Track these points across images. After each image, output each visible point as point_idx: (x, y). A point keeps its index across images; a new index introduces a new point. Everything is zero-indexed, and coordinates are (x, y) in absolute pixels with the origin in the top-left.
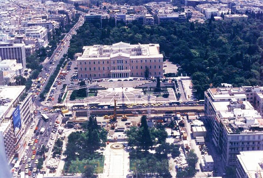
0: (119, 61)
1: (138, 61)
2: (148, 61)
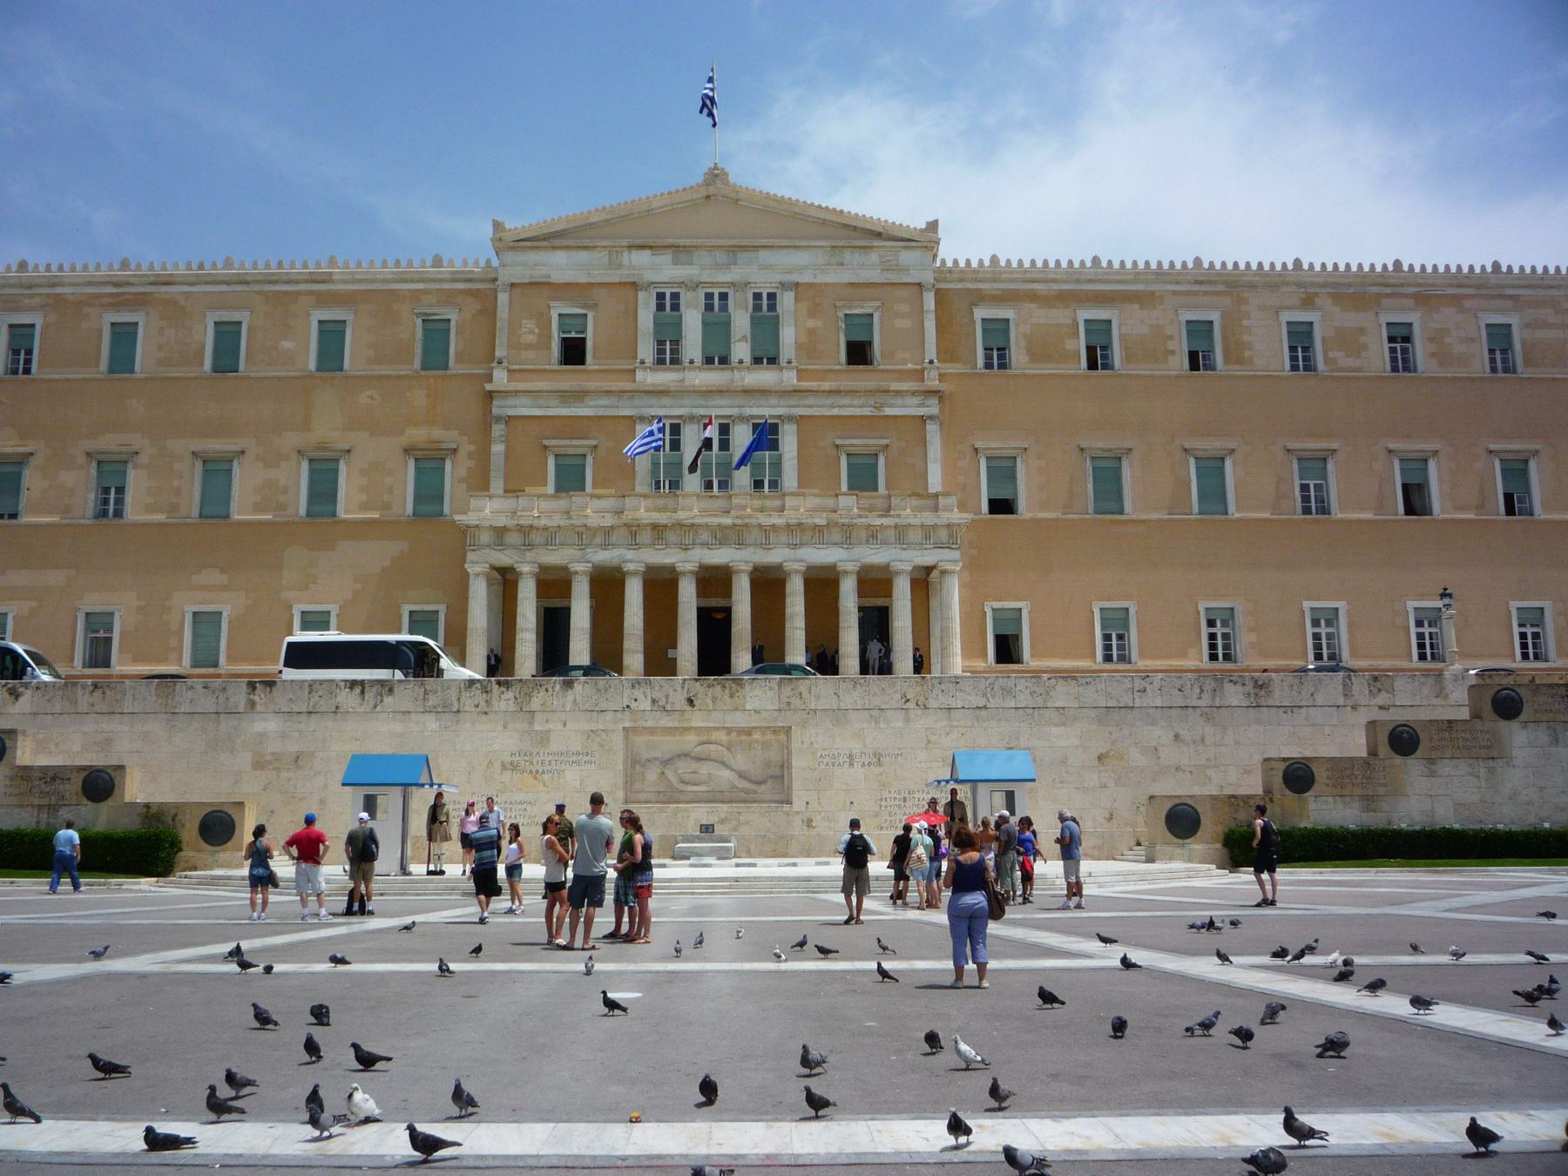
0: (692, 321)
1: (1126, 325)
2: (1349, 341)
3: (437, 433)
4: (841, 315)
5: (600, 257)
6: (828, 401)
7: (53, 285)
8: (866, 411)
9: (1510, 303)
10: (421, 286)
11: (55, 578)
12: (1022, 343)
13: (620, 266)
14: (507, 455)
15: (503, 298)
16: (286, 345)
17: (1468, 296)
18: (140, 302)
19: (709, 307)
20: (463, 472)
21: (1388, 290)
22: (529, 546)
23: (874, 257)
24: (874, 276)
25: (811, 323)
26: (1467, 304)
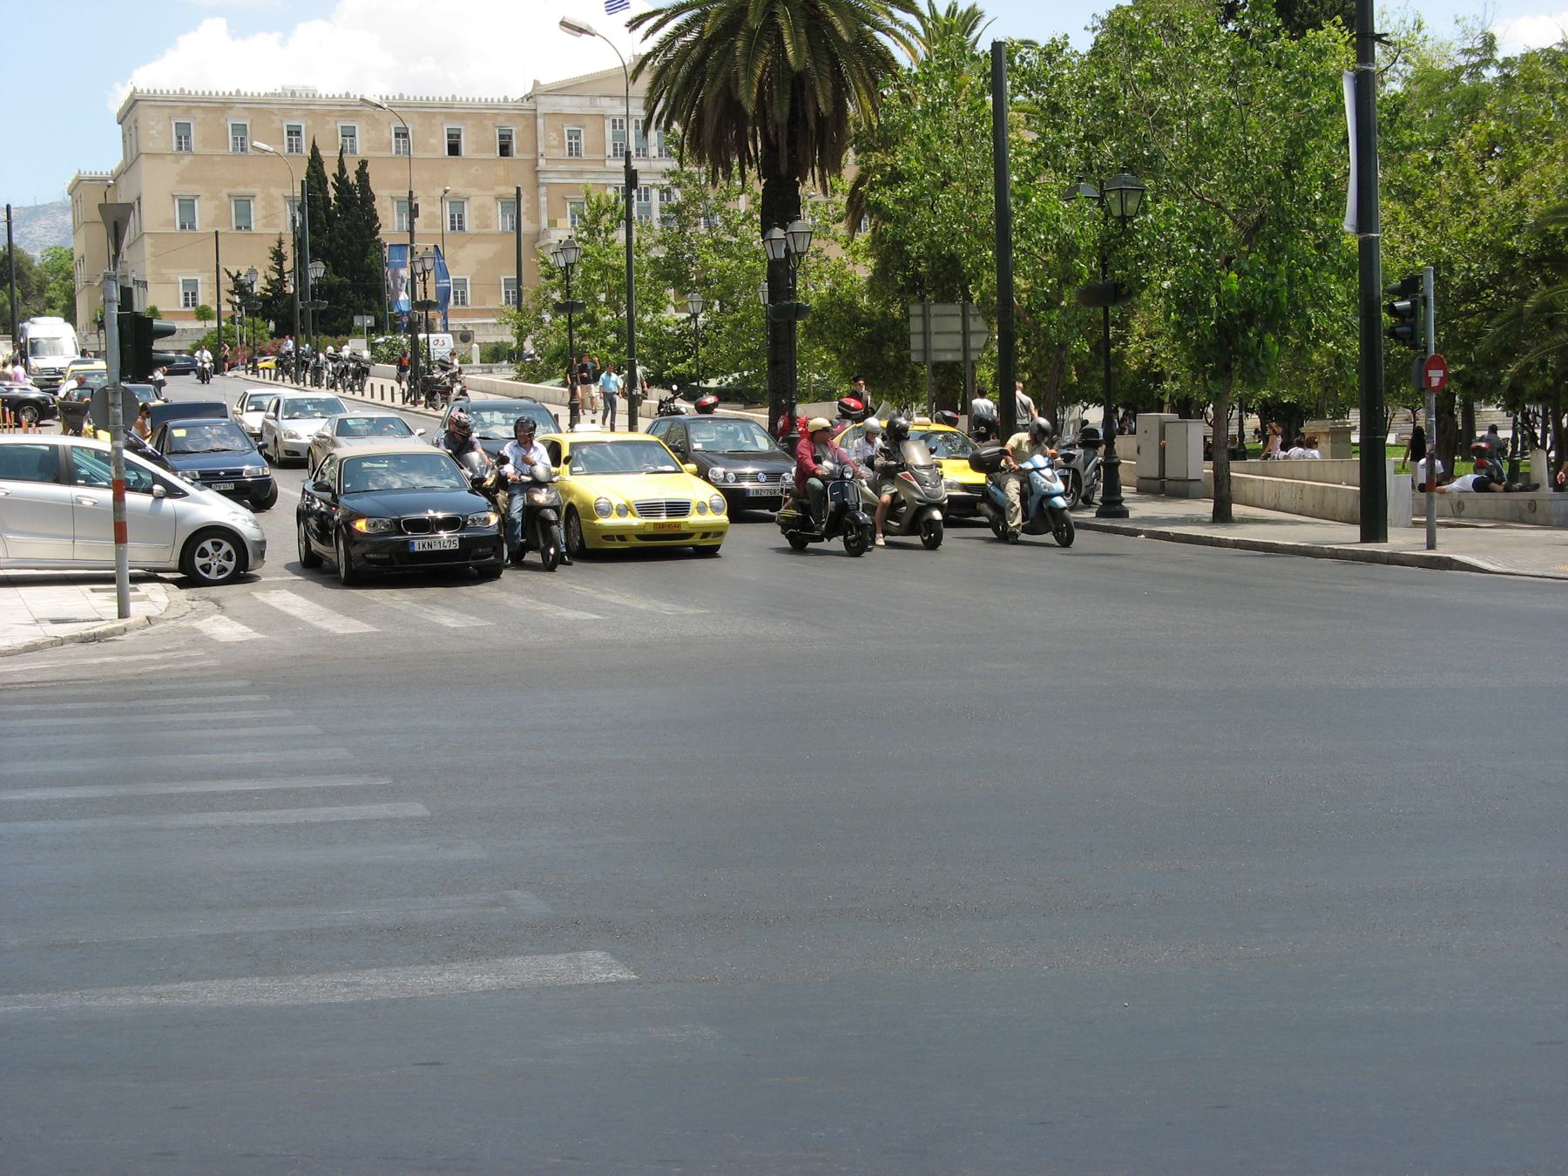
5: (586, 101)
15: (540, 121)
16: (433, 141)
18: (355, 115)
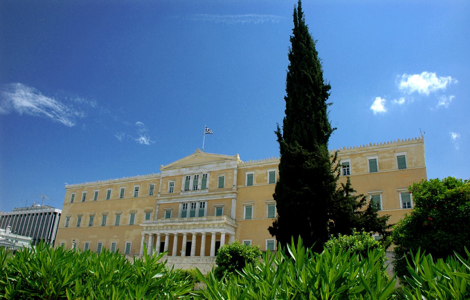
3: (150, 208)
4: (218, 177)
5: (177, 170)
6: (213, 196)
7: (101, 184)
8: (221, 198)
9: (375, 153)
10: (150, 179)
11: (95, 236)
12: (255, 179)
13: (180, 172)
14: (158, 211)
15: (161, 180)
16: (130, 192)
17: (364, 153)
18: (111, 186)
19: (195, 178)
20: (153, 215)
21: (343, 155)
22: (151, 230)
23: (225, 164)
24: (225, 168)
25: (213, 180)
26: (364, 155)
